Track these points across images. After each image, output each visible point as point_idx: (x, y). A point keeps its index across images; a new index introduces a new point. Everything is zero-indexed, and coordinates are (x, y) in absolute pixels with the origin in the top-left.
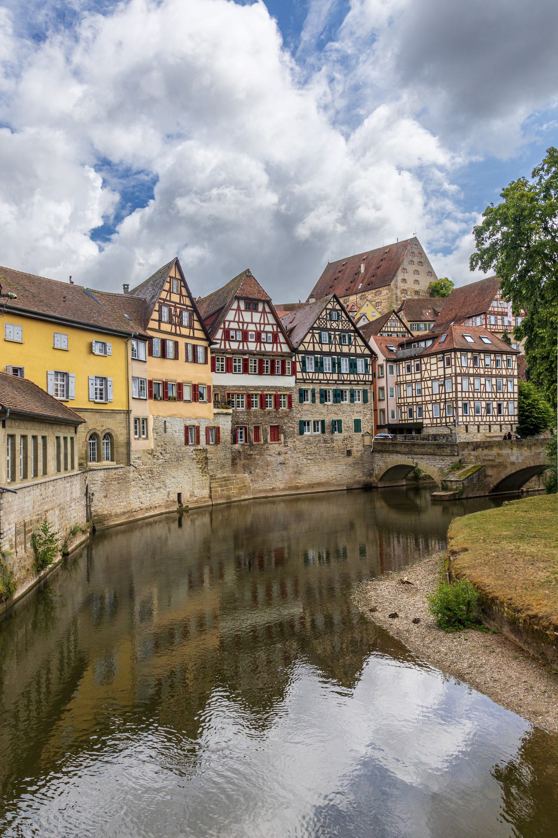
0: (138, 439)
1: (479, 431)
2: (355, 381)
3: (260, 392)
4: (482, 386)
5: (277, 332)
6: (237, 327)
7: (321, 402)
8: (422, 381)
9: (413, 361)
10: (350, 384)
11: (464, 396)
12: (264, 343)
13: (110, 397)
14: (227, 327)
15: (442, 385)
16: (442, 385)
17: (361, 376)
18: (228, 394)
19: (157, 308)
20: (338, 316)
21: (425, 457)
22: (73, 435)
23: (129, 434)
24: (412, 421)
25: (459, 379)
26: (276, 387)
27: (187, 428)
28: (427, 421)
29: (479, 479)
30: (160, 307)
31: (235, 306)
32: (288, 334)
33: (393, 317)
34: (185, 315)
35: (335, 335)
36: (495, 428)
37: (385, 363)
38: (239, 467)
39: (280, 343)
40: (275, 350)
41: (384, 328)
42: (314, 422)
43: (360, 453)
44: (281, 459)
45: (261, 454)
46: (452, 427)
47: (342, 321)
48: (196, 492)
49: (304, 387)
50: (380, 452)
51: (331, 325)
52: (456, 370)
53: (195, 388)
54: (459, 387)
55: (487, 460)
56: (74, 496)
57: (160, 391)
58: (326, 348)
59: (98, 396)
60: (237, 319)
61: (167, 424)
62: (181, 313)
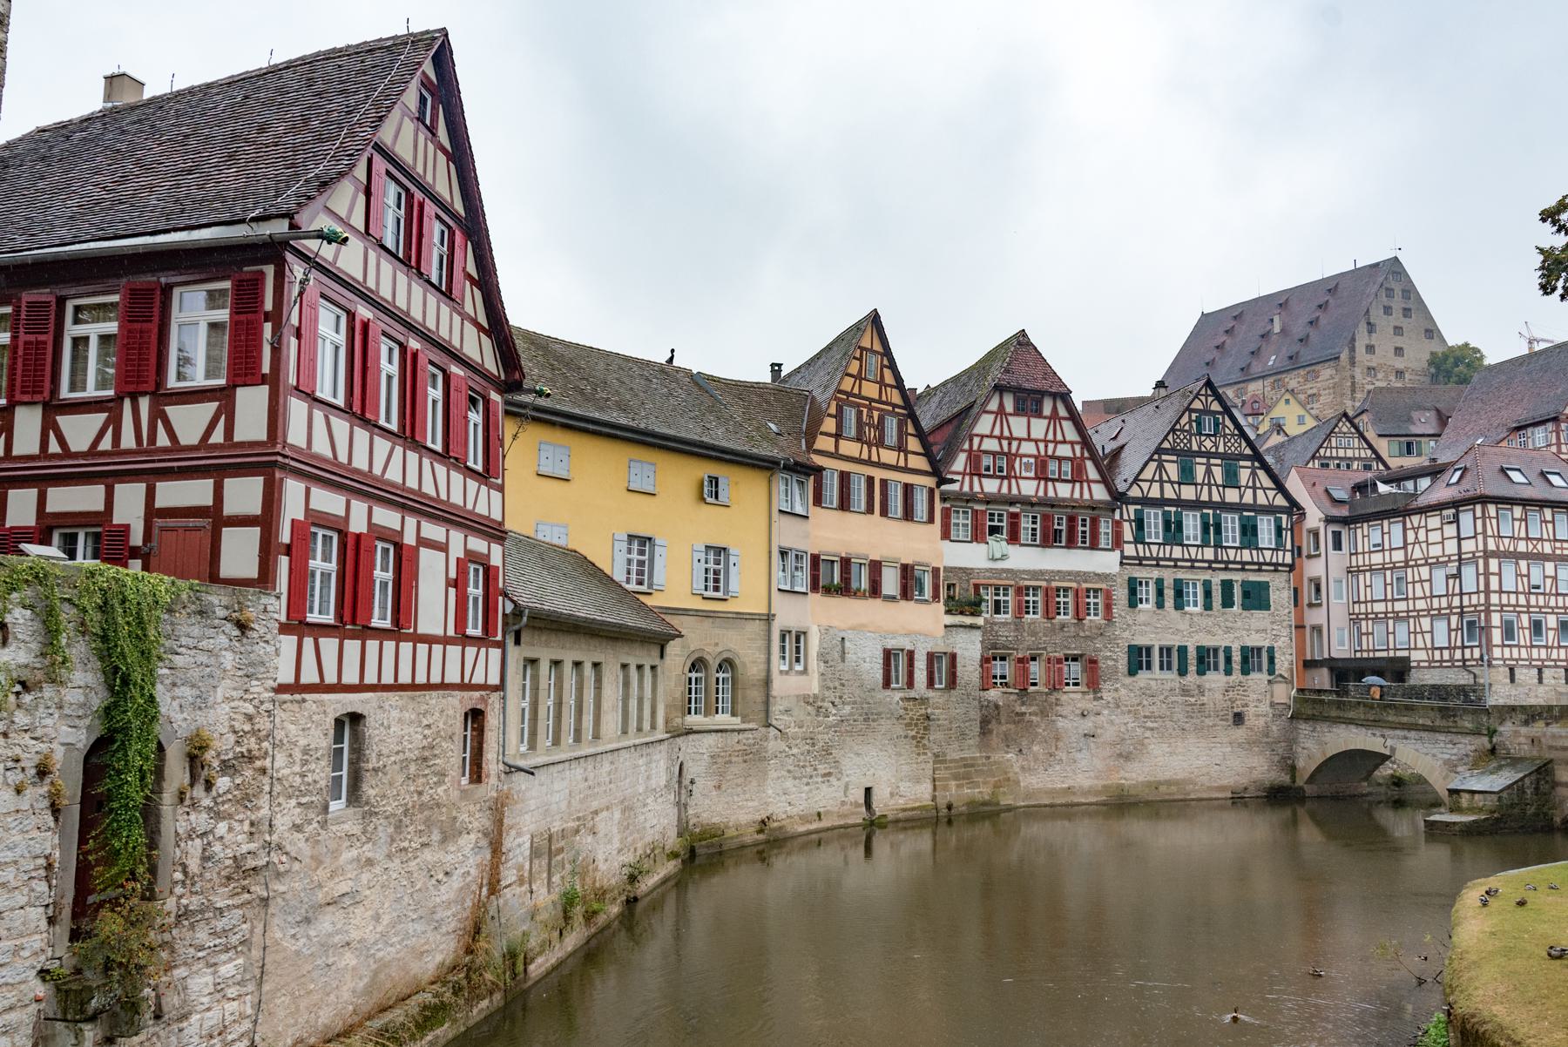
0: (787, 673)
1: (1540, 680)
2: (1252, 563)
3: (1044, 584)
4: (1549, 581)
5: (1083, 458)
6: (997, 449)
7: (1179, 606)
8: (1407, 566)
9: (1386, 523)
10: (1243, 569)
11: (1505, 601)
12: (1053, 480)
13: (733, 586)
14: (975, 447)
15: (1454, 576)
16: (1454, 576)
17: (1268, 554)
18: (977, 587)
19: (833, 410)
20: (1217, 424)
21: (1413, 734)
22: (657, 662)
23: (769, 661)
24: (1384, 654)
25: (1494, 564)
26: (1078, 573)
27: (888, 654)
28: (1417, 656)
29: (1537, 789)
30: (840, 409)
31: (993, 405)
32: (1108, 464)
33: (1345, 427)
34: (892, 425)
35: (1209, 466)
37: (1322, 525)
38: (995, 740)
39: (1089, 482)
40: (1077, 495)
41: (1322, 451)
42: (1161, 649)
43: (1262, 721)
44: (1087, 725)
45: (1043, 713)
46: (1474, 670)
47: (1225, 435)
48: (905, 787)
49: (1139, 573)
50: (1307, 719)
51: (1201, 444)
52: (1485, 544)
53: (906, 571)
54: (1494, 581)
55: (1556, 749)
56: (653, 783)
57: (834, 577)
58: (1188, 493)
59: (711, 584)
60: (997, 432)
61: (847, 644)
62: (881, 419)
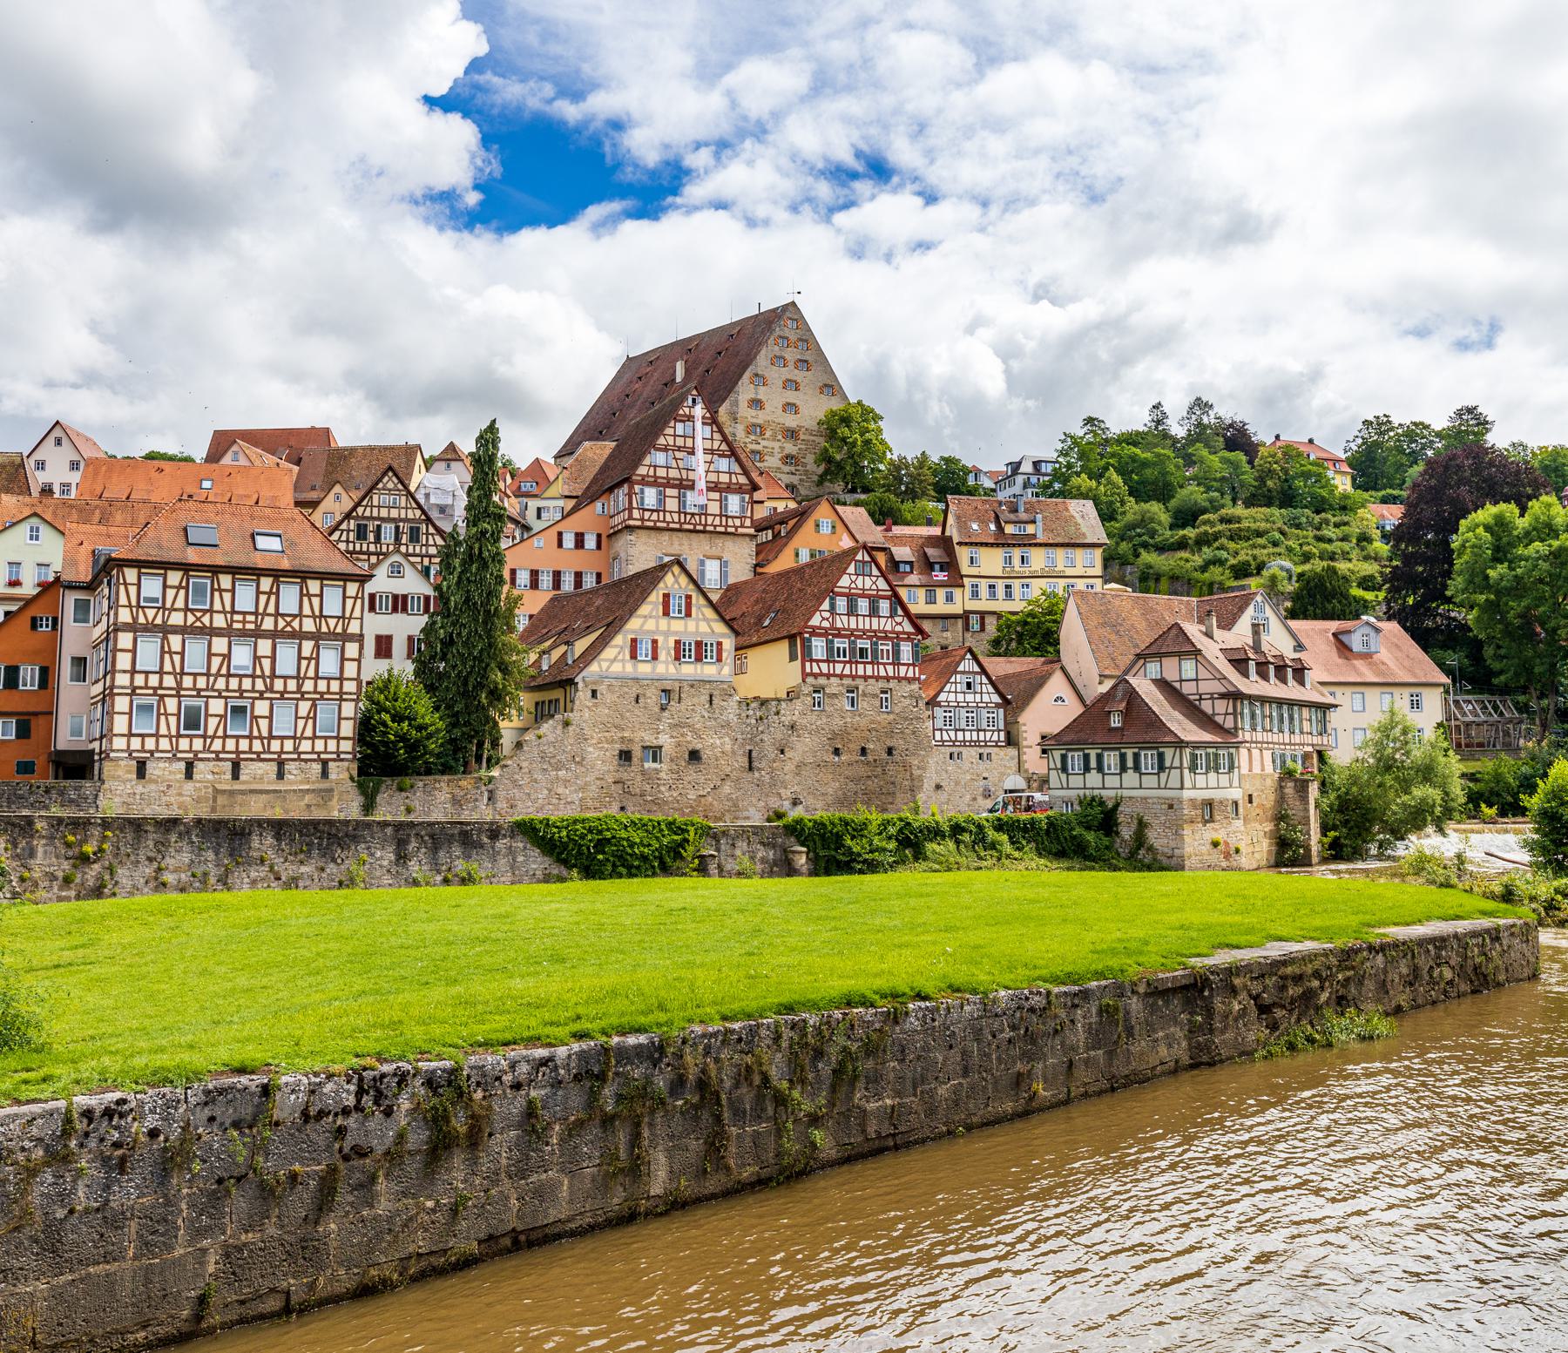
1: (189, 774)
36: (258, 773)
